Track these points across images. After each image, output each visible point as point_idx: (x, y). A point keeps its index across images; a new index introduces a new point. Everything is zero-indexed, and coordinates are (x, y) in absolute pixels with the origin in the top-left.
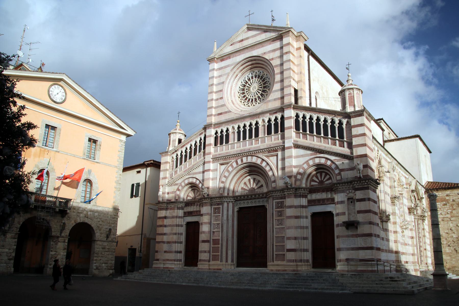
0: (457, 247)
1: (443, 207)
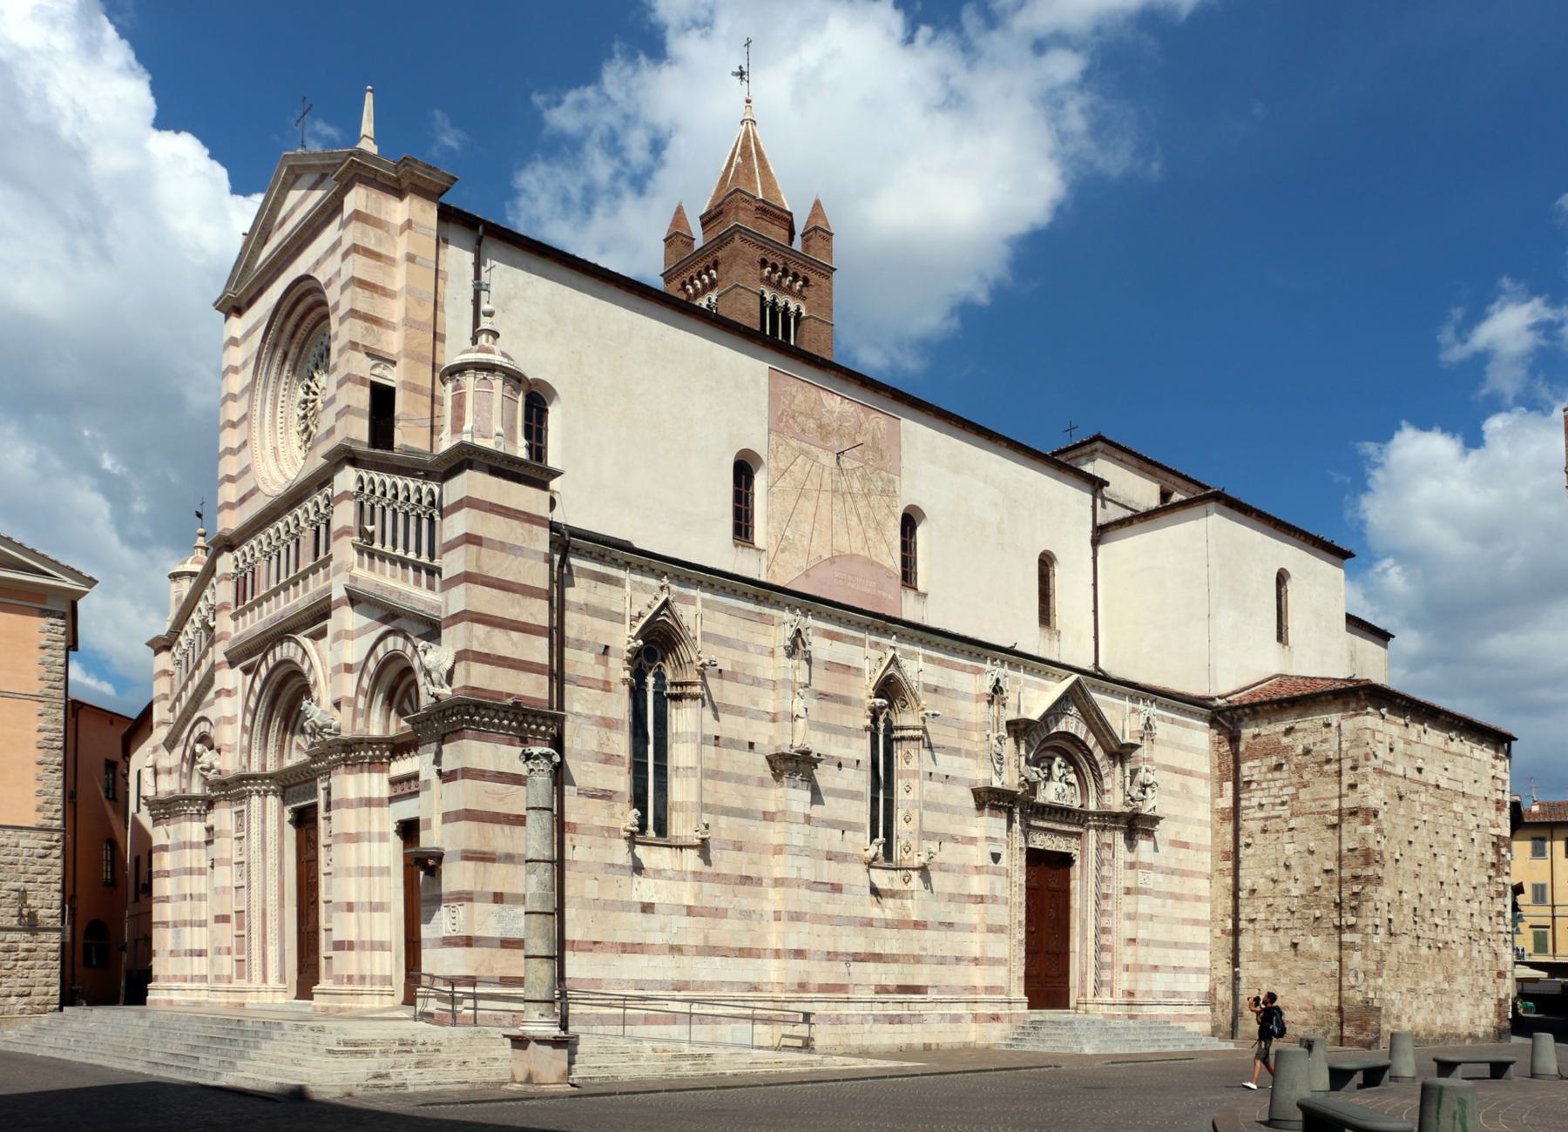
0: (1299, 933)
1: (1269, 776)
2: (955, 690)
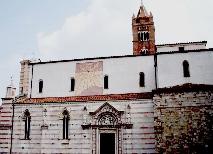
2: (78, 110)
